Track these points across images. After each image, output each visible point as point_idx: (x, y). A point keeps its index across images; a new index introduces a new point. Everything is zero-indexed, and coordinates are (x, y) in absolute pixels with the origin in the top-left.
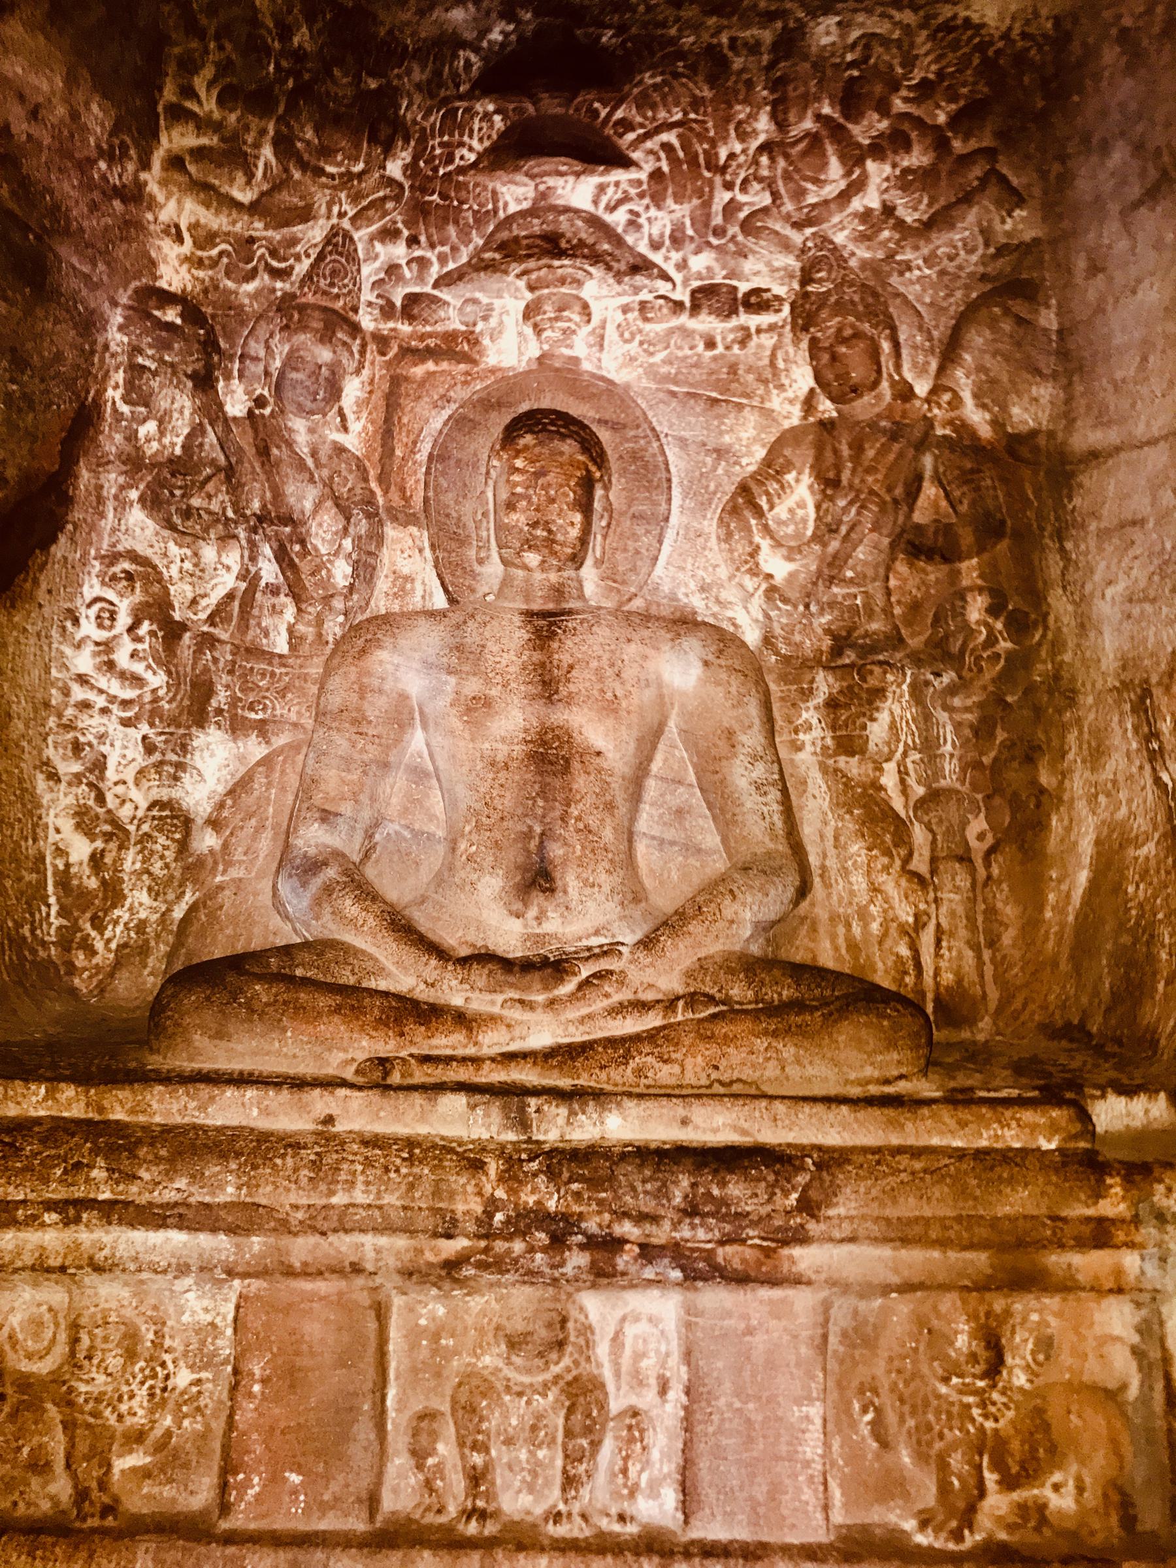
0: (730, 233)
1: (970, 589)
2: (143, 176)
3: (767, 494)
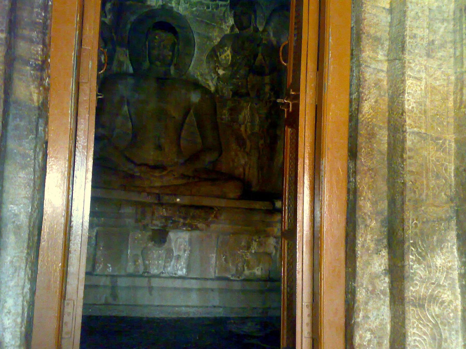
1: (267, 84)
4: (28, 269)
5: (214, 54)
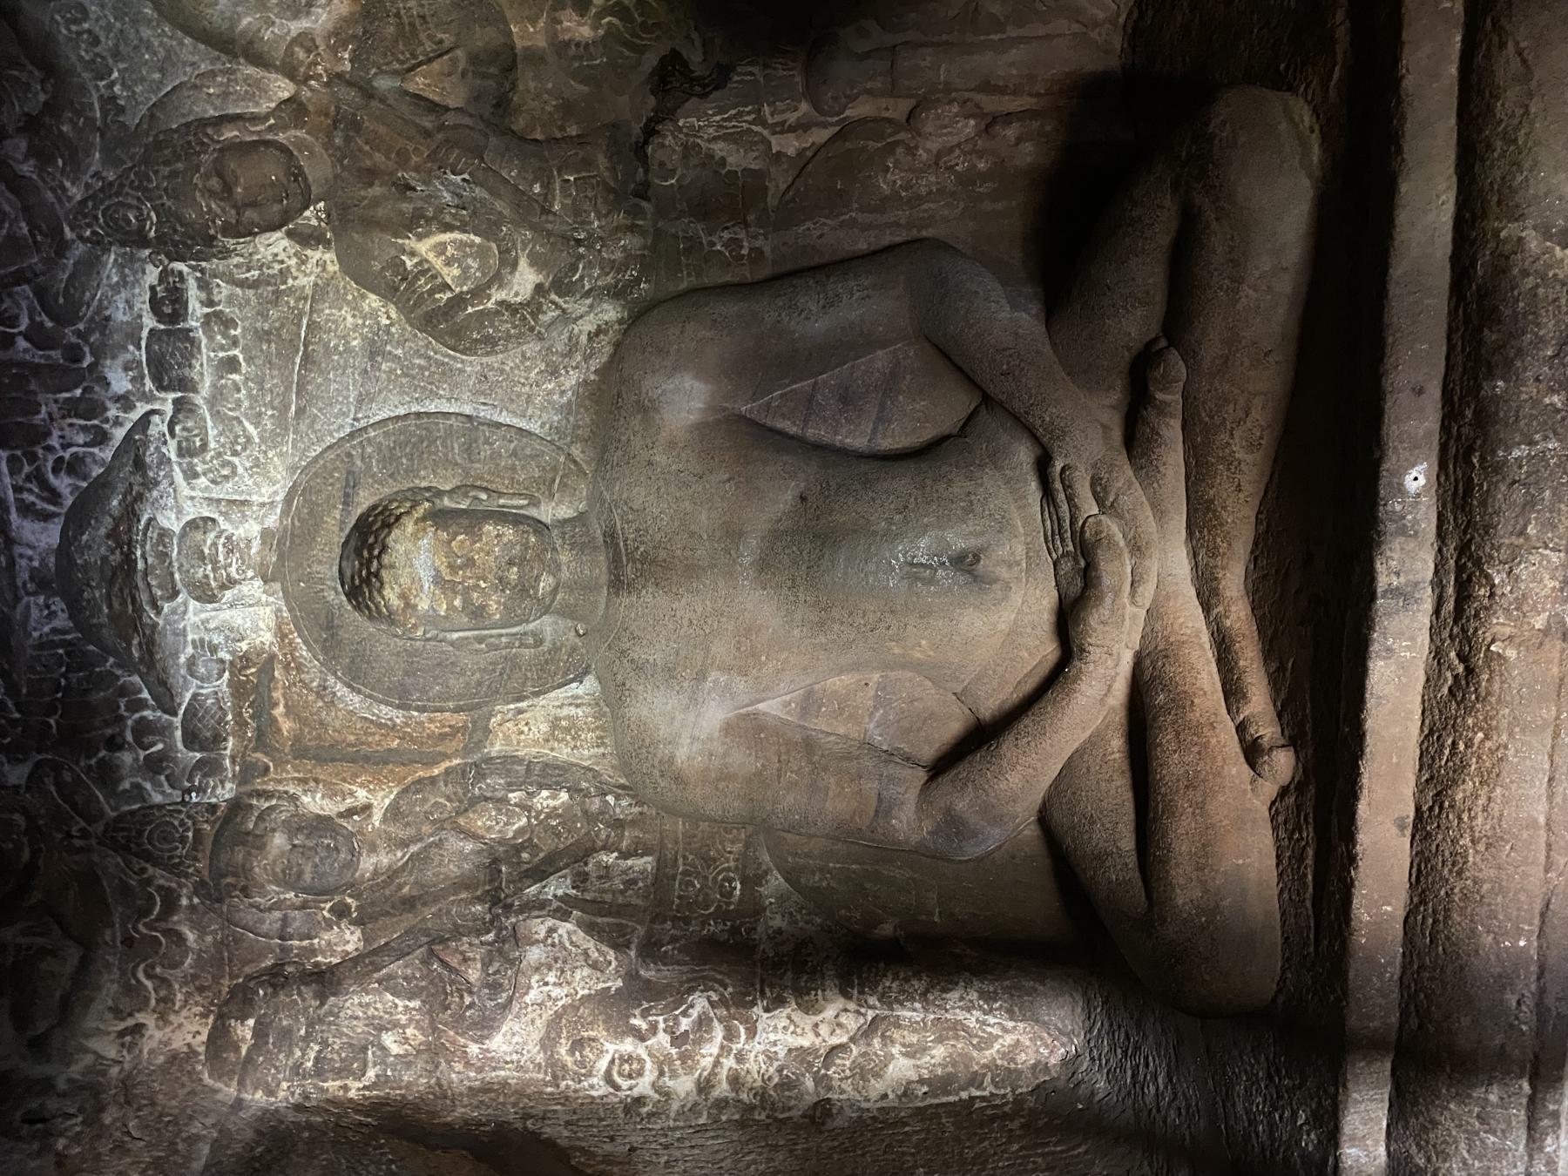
0: (74, 340)
2: (62, 1085)
3: (432, 292)
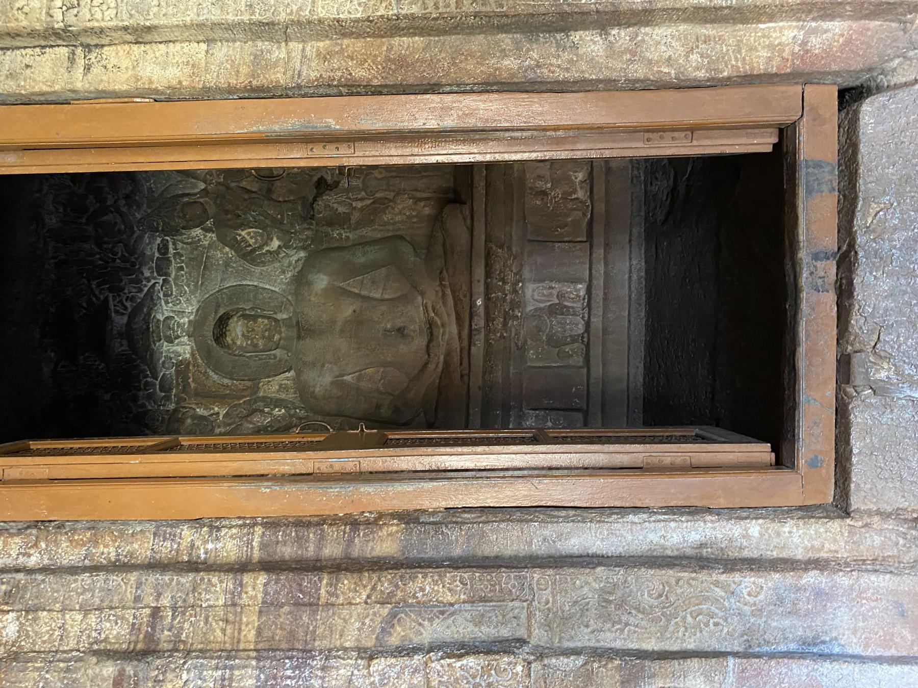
4: (610, 520)
5: (249, 256)
